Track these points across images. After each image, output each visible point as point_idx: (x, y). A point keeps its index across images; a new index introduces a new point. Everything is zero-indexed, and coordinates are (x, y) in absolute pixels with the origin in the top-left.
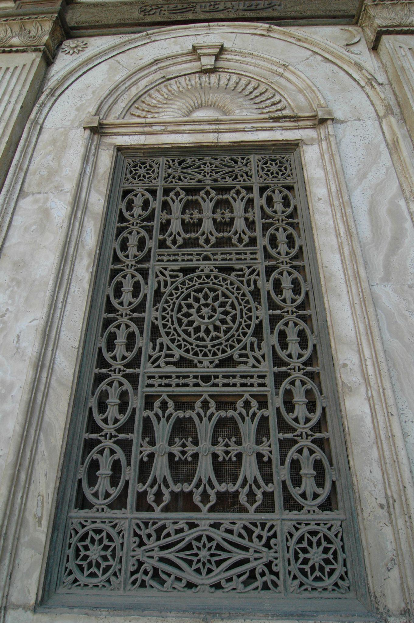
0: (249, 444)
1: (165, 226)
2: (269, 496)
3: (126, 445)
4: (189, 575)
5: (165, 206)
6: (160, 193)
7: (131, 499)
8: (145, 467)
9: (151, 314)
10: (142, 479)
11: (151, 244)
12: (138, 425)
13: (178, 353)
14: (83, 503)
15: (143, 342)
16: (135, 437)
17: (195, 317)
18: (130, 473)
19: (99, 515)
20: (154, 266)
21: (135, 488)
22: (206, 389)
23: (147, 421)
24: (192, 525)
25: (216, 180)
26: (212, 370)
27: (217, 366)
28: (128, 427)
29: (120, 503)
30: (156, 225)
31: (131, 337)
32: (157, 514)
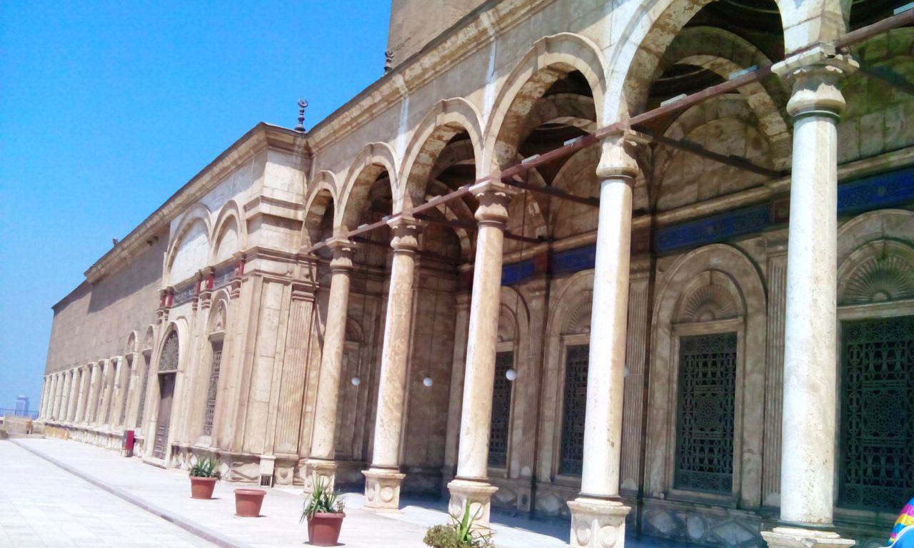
0: (897, 464)
1: (867, 367)
2: (902, 483)
3: (859, 464)
4: (878, 502)
5: (867, 356)
6: (864, 347)
7: (862, 482)
8: (865, 471)
9: (864, 413)
10: (865, 475)
11: (862, 378)
12: (862, 456)
13: (874, 430)
14: (848, 481)
15: (862, 425)
16: (862, 461)
17: (881, 417)
18: (861, 473)
19: (853, 485)
20: (864, 390)
21: (862, 477)
22: (884, 446)
23: (865, 457)
24: (879, 489)
25: (888, 338)
26: (886, 438)
27: (888, 436)
28: (859, 458)
29: (858, 482)
30: (863, 367)
31: (857, 424)
32: (869, 486)
